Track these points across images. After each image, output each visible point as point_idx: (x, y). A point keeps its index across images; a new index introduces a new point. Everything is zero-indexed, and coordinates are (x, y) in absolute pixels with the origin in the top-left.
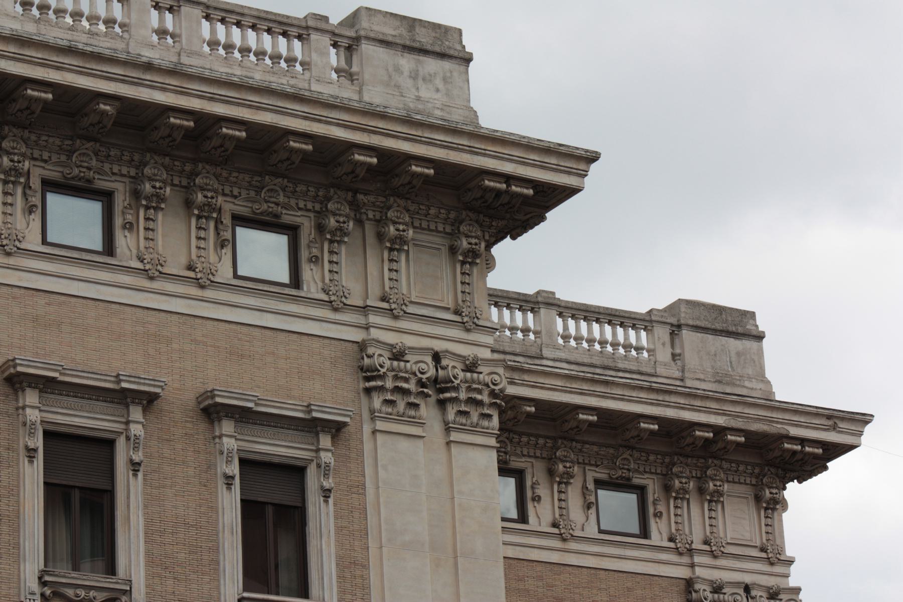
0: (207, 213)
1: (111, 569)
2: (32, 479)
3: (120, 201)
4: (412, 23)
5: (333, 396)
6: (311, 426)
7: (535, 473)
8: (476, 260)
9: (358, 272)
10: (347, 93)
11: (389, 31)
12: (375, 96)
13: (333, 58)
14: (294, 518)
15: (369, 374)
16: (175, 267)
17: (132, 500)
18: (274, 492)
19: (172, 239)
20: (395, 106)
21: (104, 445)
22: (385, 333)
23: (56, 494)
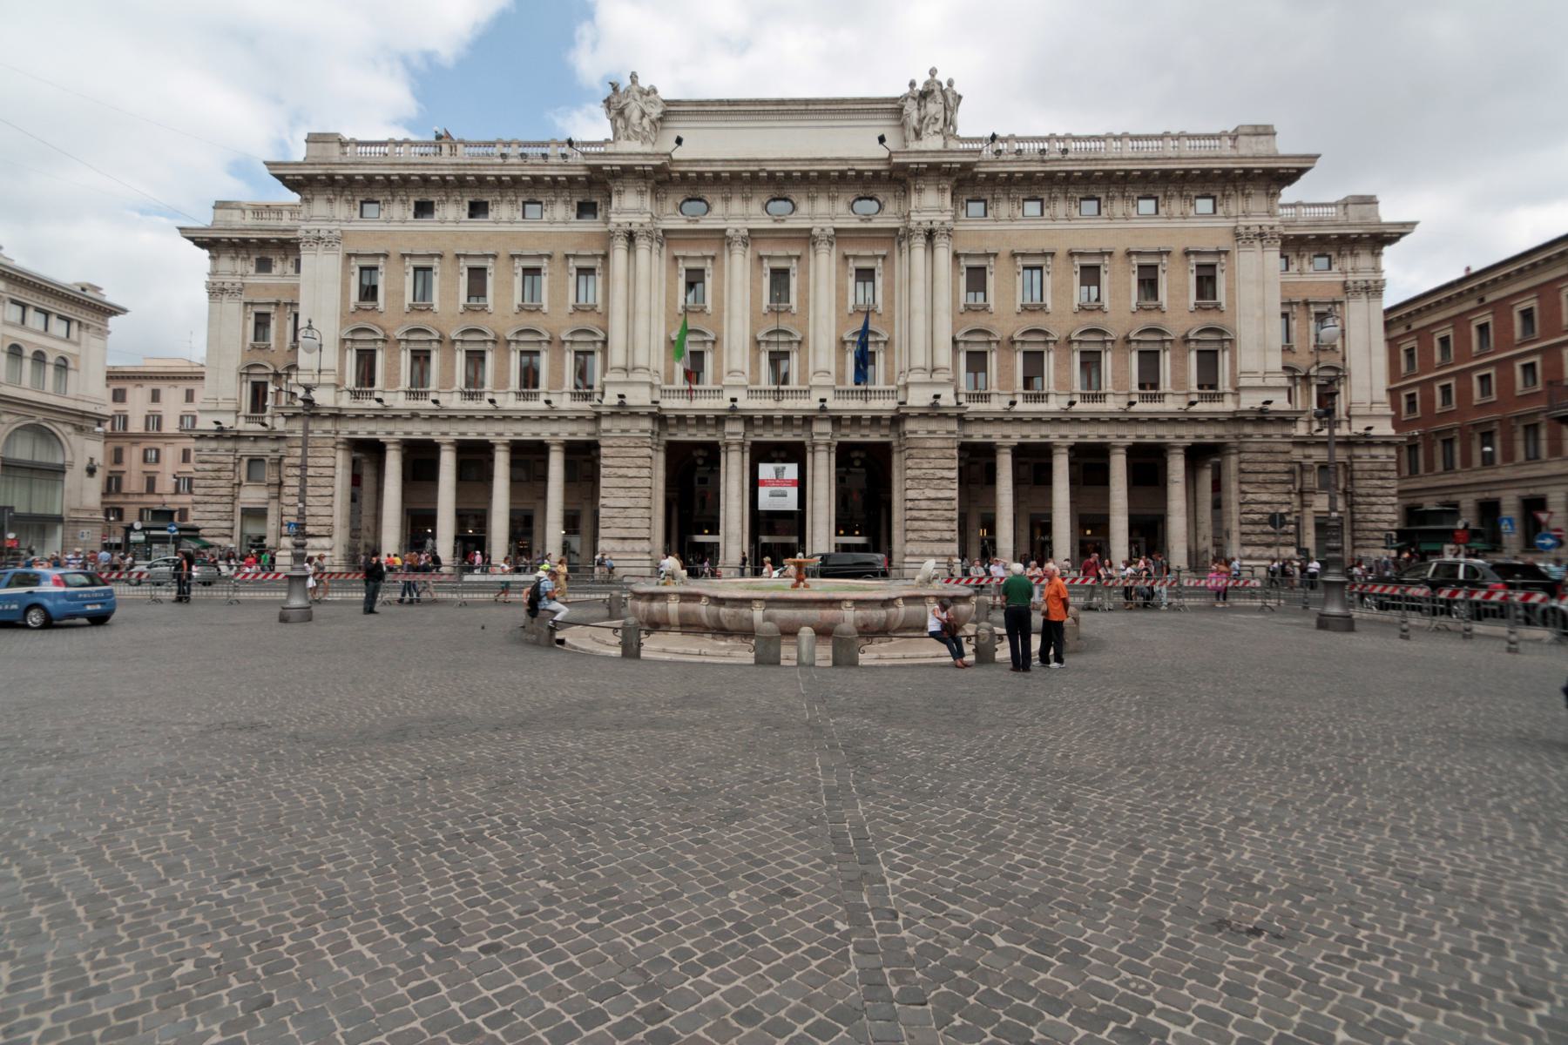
0: (1188, 197)
2: (1134, 279)
4: (1256, 127)
5: (1225, 243)
7: (1292, 256)
8: (1276, 195)
9: (1235, 206)
10: (1234, 153)
11: (1248, 130)
12: (1243, 152)
13: (1229, 143)
14: (1212, 279)
15: (1237, 235)
16: (1177, 214)
17: (1163, 281)
18: (1207, 273)
19: (1176, 206)
20: (1249, 153)
21: (1155, 267)
22: (1243, 222)
23: (1141, 282)
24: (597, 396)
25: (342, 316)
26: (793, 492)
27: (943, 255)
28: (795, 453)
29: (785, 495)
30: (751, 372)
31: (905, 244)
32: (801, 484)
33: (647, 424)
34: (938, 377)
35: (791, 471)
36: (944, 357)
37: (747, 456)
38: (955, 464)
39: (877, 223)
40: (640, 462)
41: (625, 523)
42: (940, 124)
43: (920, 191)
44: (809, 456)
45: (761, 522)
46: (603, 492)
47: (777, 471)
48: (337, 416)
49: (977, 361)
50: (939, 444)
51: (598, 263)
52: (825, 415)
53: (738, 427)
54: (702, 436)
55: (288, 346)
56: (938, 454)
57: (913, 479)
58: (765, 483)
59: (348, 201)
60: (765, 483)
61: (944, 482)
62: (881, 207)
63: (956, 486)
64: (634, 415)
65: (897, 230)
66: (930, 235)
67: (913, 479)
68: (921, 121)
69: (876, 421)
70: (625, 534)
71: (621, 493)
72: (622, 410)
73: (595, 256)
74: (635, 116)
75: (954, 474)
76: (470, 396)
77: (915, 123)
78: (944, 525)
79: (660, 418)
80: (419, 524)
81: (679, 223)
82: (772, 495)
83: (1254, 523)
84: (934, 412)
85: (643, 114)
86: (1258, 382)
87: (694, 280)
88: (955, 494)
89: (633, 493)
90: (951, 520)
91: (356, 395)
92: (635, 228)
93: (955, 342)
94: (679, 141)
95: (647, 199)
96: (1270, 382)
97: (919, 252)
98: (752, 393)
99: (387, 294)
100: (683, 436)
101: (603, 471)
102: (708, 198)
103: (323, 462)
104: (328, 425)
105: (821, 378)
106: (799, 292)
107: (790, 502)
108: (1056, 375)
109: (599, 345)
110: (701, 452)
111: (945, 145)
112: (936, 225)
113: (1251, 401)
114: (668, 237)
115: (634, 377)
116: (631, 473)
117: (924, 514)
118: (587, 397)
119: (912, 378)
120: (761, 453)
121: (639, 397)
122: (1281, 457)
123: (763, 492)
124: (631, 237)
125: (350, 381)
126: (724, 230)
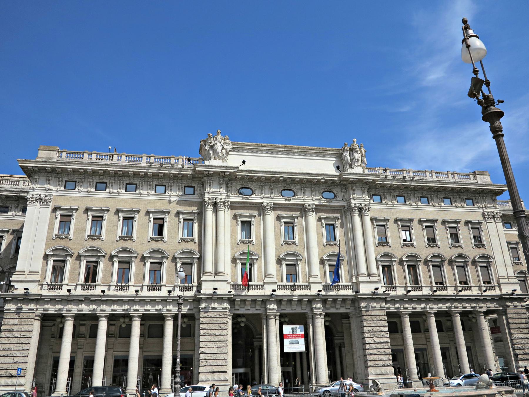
1: (459, 242)
3: (452, 199)
5: (481, 219)
6: (479, 223)
12: (479, 182)
15: (484, 215)
24: (195, 289)
25: (47, 241)
26: (302, 341)
27: (367, 219)
28: (303, 320)
29: (298, 343)
31: (348, 213)
32: (306, 336)
33: (226, 305)
34: (373, 279)
36: (374, 270)
37: (278, 321)
38: (386, 324)
39: (335, 203)
41: (212, 362)
42: (360, 163)
43: (354, 191)
45: (287, 358)
46: (201, 344)
47: (293, 330)
48: (39, 300)
49: (387, 270)
50: (377, 313)
51: (195, 217)
52: (319, 299)
55: (11, 256)
56: (378, 318)
57: (368, 332)
58: (288, 337)
59: (59, 181)
60: (288, 337)
61: (383, 334)
62: (335, 196)
63: (388, 335)
64: (220, 299)
65: (344, 207)
66: (361, 210)
67: (367, 332)
68: (351, 160)
70: (215, 369)
71: (212, 344)
72: (214, 297)
73: (193, 213)
74: (219, 149)
75: (386, 329)
76: (122, 288)
77: (349, 161)
78: (386, 357)
79: (232, 302)
80: (119, 366)
81: (239, 199)
82: (291, 344)
83: (520, 349)
84: (374, 297)
85: (223, 148)
86: (506, 281)
87: (246, 225)
88: (388, 340)
89: (220, 344)
90: (388, 354)
91: (51, 287)
92: (218, 200)
93: (377, 261)
94: (244, 162)
95: (224, 186)
96: (512, 281)
97: (357, 219)
98: (281, 287)
99: (75, 229)
101: (202, 332)
102: (252, 187)
103: (26, 328)
104: (32, 306)
105: (314, 280)
106: (299, 235)
108: (424, 277)
109: (196, 260)
110: (244, 319)
111: (364, 171)
112: (363, 205)
113: (507, 290)
114: (233, 206)
115: (218, 278)
116: (218, 332)
117: (375, 351)
118: (190, 289)
119: (361, 279)
120: (285, 319)
121: (224, 289)
122: (523, 316)
123: (286, 341)
124: (215, 205)
125: (48, 279)
126: (262, 203)
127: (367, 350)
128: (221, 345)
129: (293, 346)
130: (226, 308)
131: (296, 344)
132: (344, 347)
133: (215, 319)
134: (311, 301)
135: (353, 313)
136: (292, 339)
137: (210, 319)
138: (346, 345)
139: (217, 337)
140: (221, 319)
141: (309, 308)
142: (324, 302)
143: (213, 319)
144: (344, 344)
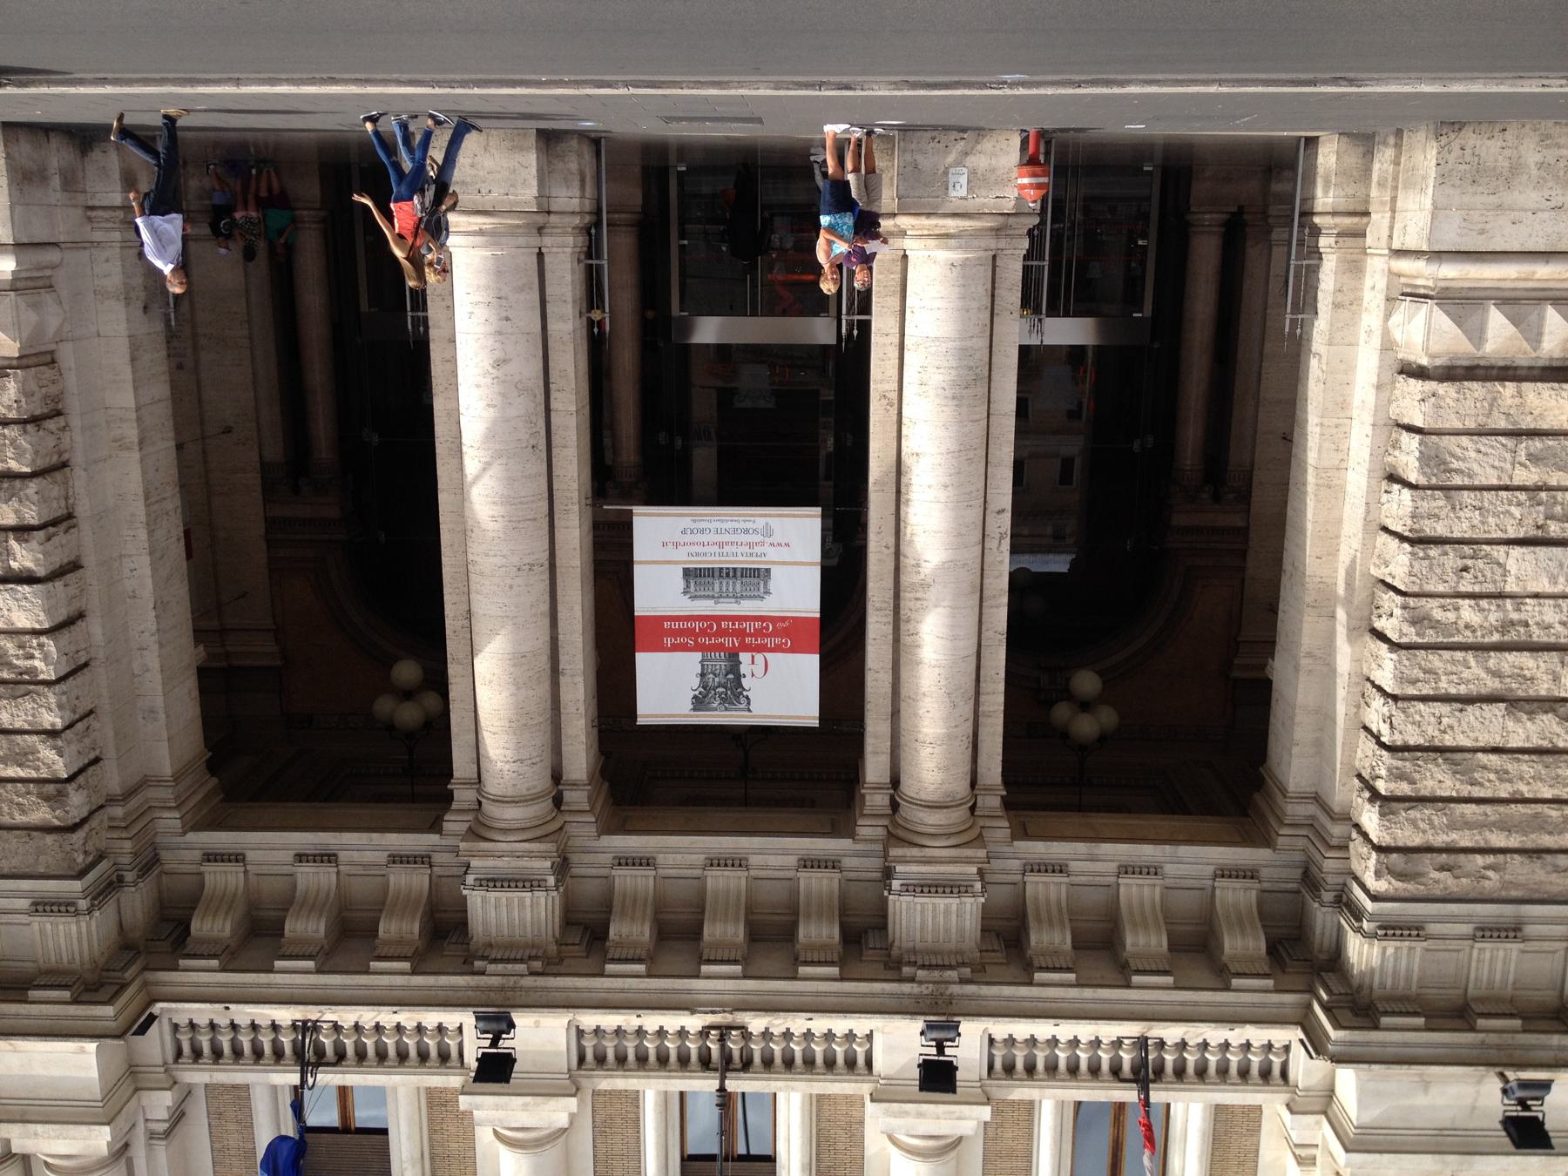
26: (657, 591)
28: (649, 773)
29: (695, 576)
30: (855, 1130)
32: (617, 634)
35: (666, 689)
37: (875, 768)
40: (1437, 779)
44: (579, 758)
47: (734, 690)
53: (918, 917)
54: (1093, 863)
58: (786, 634)
60: (786, 634)
69: (260, 936)
82: (756, 577)
100: (1191, 863)
107: (667, 541)
123: (798, 591)
127: (31, 516)
128: (1468, 612)
129: (738, 557)
130: (1390, 929)
131: (711, 573)
132: (265, 467)
133: (1498, 840)
134: (585, 937)
135: (170, 821)
136: (748, 607)
137: (1547, 841)
138: (254, 479)
139: (1491, 685)
140: (1440, 840)
141: (584, 865)
142: (445, 937)
143: (1514, 841)
144: (269, 489)
